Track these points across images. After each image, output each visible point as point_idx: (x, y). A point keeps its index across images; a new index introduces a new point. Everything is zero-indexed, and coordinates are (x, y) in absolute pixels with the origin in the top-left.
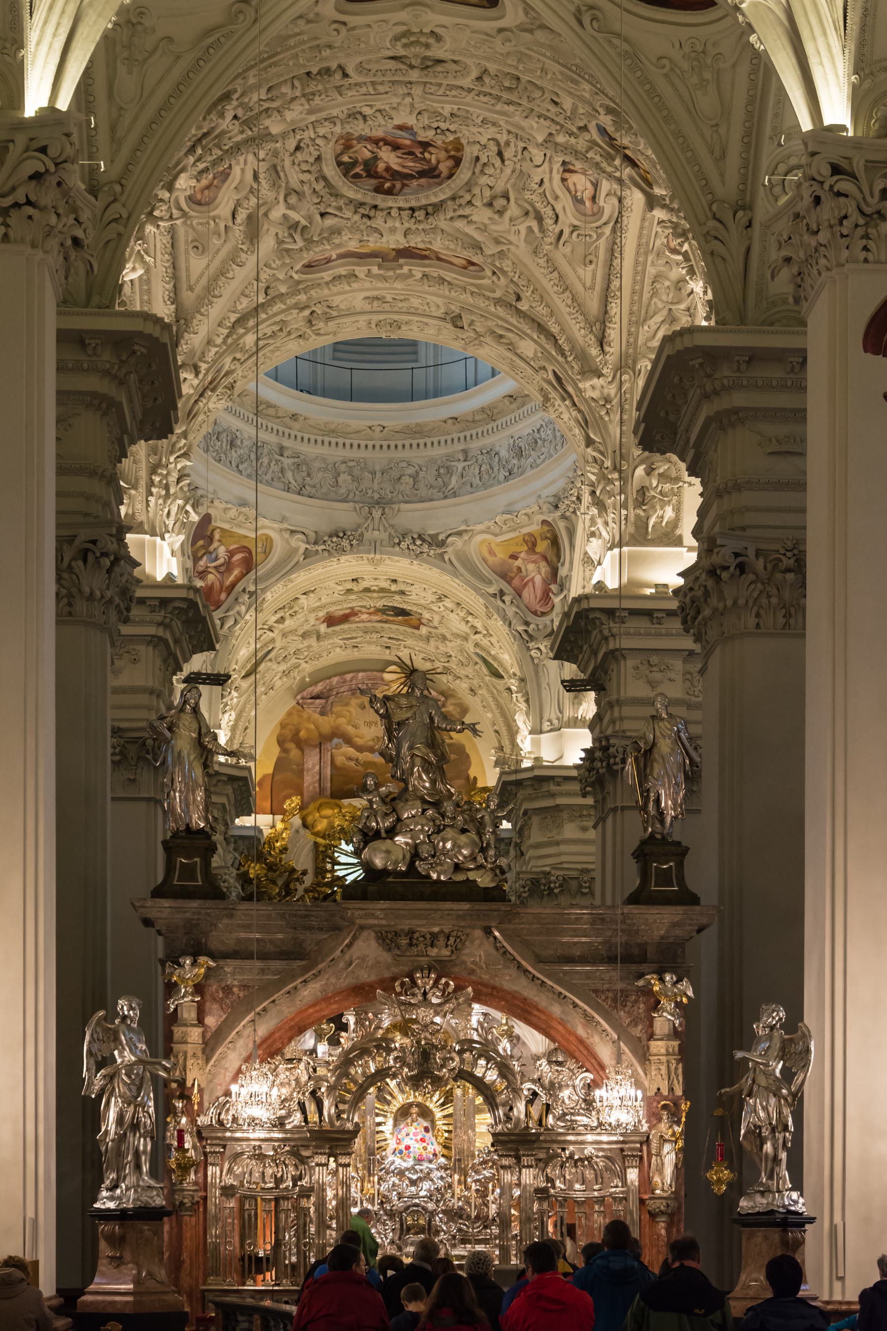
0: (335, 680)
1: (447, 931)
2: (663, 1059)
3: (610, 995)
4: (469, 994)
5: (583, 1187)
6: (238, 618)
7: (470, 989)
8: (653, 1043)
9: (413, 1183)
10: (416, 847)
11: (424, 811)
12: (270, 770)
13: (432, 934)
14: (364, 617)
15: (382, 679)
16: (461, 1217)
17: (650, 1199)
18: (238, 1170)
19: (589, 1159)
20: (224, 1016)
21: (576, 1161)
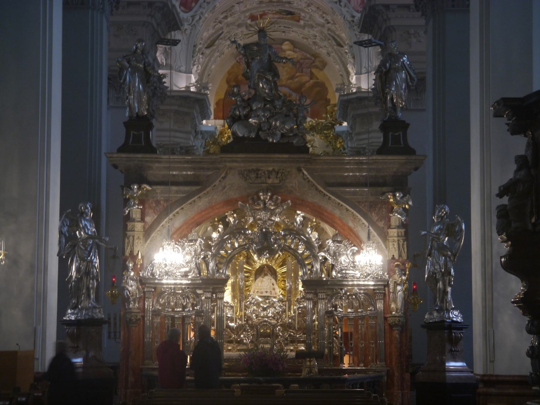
1: (276, 169)
2: (396, 239)
3: (367, 204)
4: (288, 204)
5: (353, 311)
6: (201, 16)
7: (289, 201)
8: (390, 230)
9: (264, 309)
10: (260, 124)
11: (265, 105)
13: (268, 171)
14: (270, 16)
15: (281, 49)
16: (290, 328)
17: (390, 317)
18: (162, 301)
19: (356, 294)
20: (156, 217)
21: (349, 296)
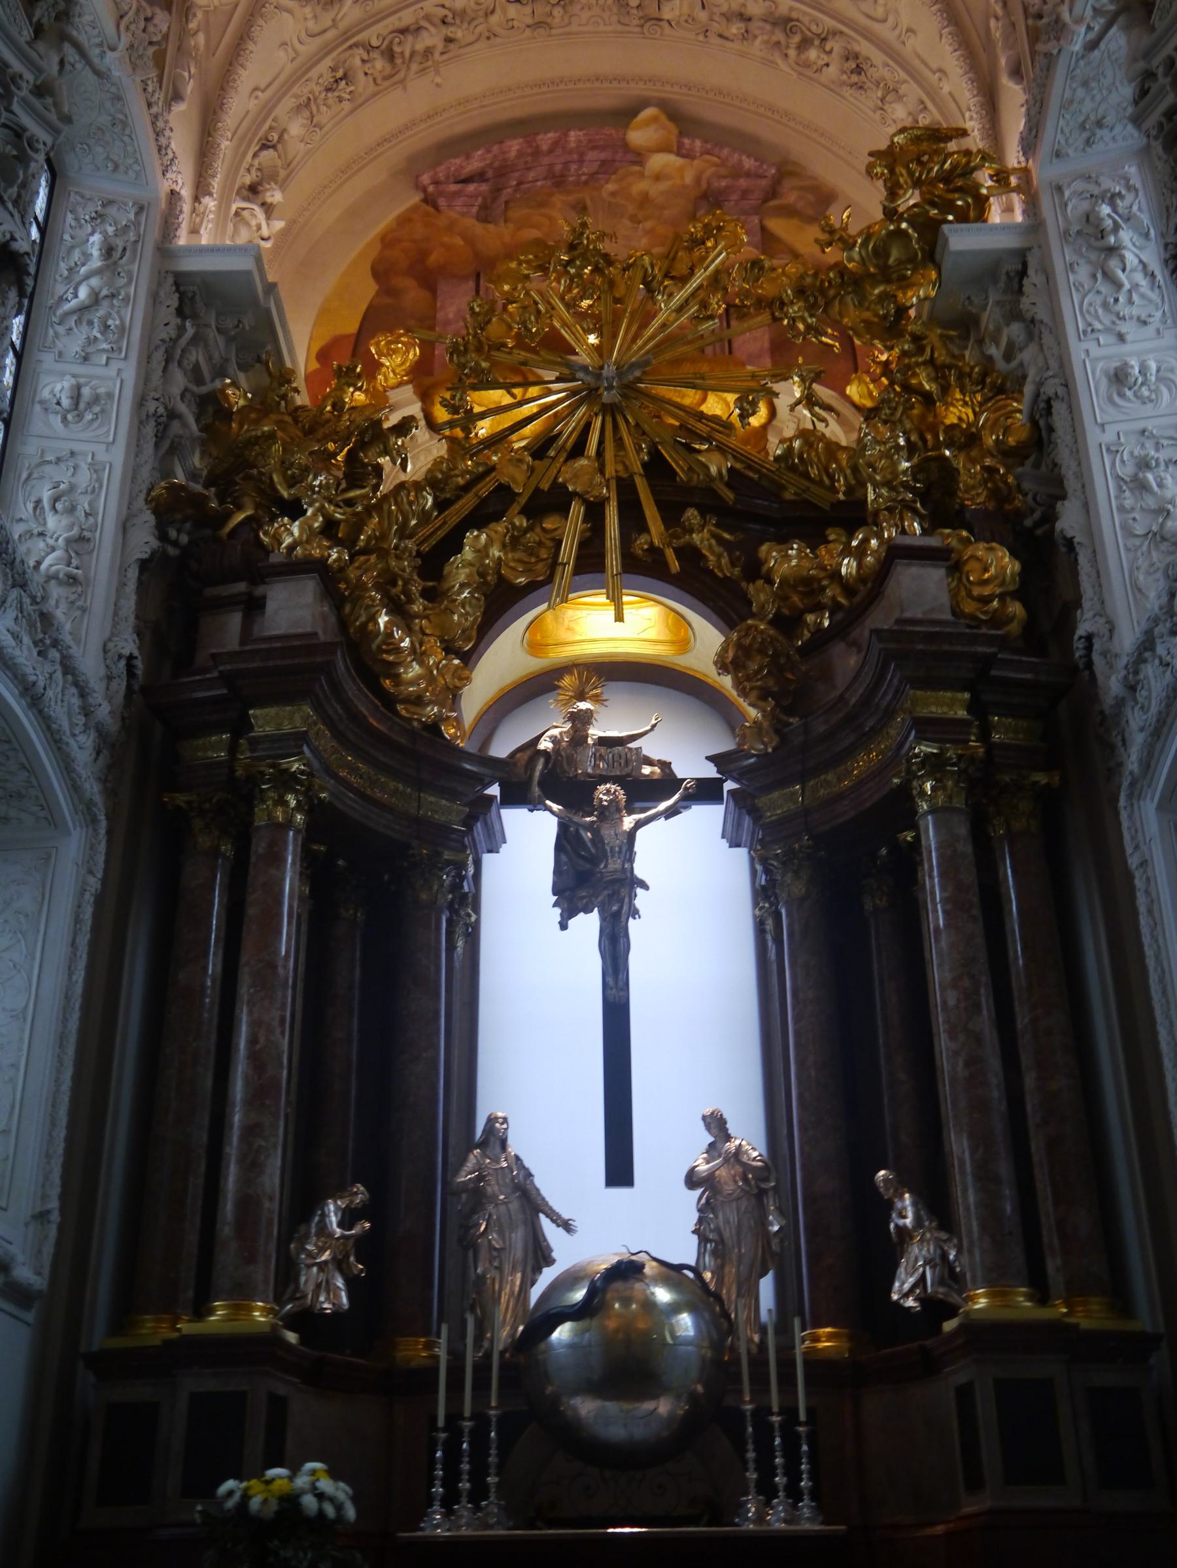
0: (514, 147)
12: (352, 327)
15: (625, 146)
